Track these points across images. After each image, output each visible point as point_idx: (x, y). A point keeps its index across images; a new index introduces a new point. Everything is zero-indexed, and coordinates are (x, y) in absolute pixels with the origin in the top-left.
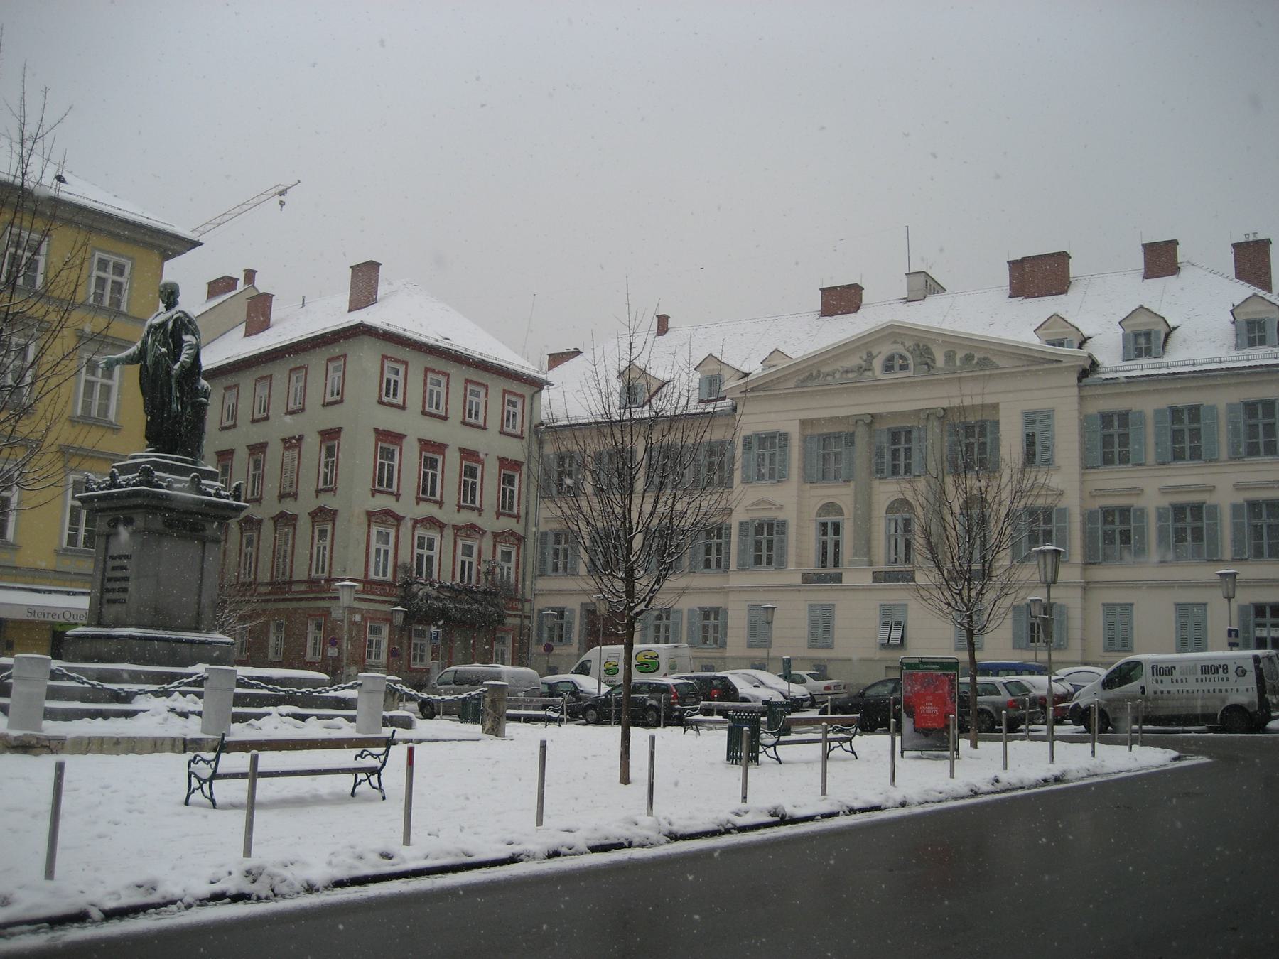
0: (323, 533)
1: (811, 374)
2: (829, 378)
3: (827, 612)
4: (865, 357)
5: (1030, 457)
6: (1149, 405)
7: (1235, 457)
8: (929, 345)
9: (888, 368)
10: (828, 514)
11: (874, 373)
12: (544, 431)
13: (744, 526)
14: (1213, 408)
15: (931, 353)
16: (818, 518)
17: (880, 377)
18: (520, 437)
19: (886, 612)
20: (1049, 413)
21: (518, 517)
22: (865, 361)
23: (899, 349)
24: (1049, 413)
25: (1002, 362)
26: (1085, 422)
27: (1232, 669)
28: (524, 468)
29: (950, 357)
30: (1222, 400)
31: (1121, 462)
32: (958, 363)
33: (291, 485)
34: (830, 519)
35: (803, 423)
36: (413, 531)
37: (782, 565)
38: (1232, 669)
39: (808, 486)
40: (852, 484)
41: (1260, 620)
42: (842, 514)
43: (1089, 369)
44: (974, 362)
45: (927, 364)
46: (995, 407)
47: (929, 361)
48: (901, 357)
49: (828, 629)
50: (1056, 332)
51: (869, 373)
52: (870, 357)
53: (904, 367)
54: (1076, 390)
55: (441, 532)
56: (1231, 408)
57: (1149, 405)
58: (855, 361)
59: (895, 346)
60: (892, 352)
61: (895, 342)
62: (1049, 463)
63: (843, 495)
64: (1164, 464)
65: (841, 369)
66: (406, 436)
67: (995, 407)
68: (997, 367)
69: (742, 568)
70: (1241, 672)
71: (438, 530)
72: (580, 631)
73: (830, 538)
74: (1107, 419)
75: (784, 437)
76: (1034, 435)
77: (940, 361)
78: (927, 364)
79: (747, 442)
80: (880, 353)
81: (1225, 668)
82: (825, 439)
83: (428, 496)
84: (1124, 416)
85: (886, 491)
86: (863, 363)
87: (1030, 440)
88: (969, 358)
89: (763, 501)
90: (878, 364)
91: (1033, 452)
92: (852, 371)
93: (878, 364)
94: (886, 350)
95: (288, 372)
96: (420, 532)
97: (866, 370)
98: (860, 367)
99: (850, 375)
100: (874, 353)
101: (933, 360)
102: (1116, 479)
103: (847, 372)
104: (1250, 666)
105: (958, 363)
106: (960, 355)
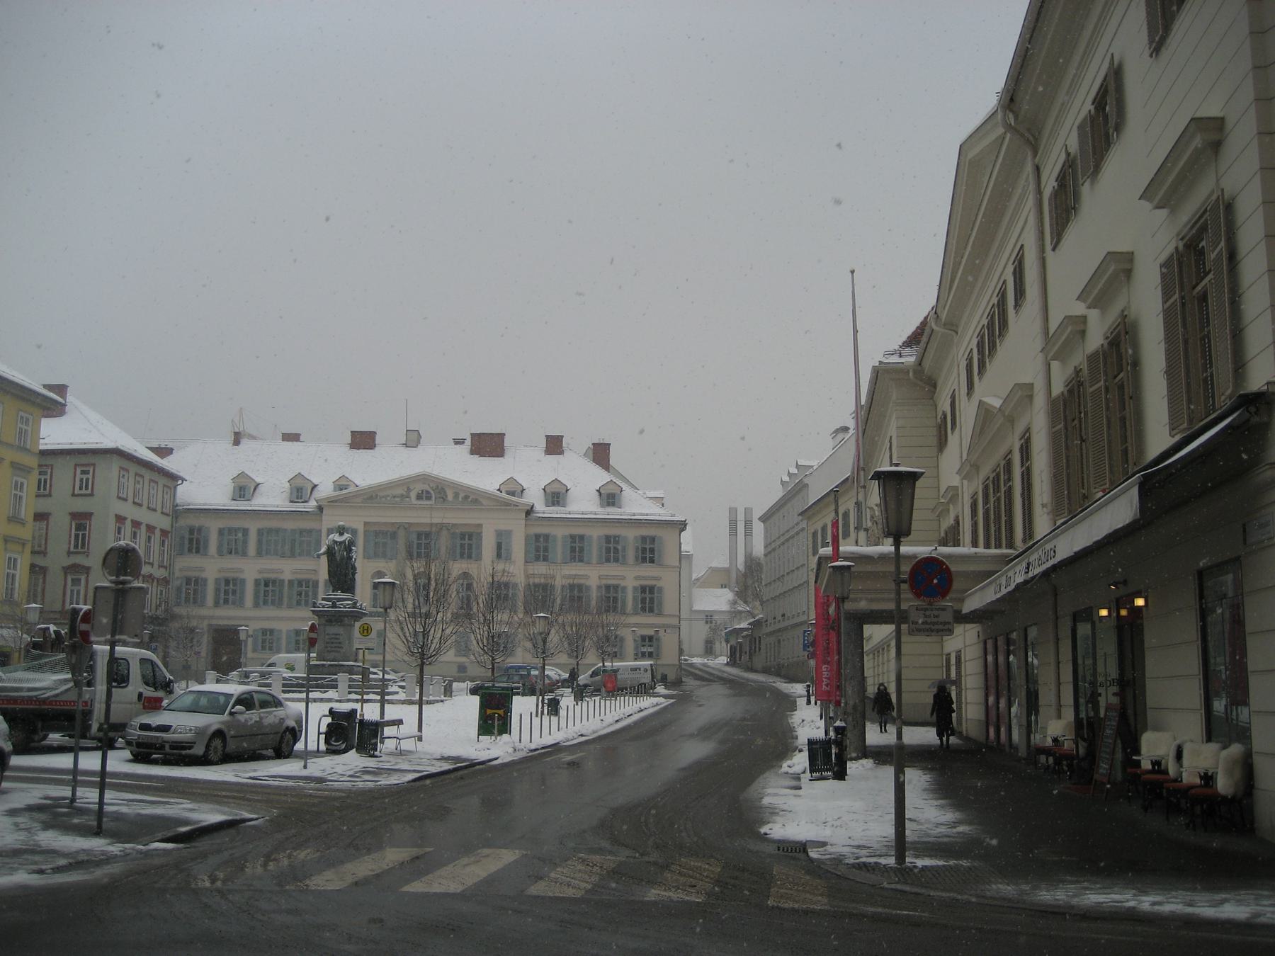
0: (76, 582)
2: (384, 499)
4: (406, 490)
5: (499, 556)
6: (560, 532)
7: (600, 563)
8: (446, 489)
9: (419, 497)
12: (177, 513)
14: (591, 537)
15: (445, 492)
17: (416, 502)
18: (168, 515)
20: (509, 533)
21: (166, 568)
23: (426, 487)
24: (509, 533)
25: (484, 502)
26: (527, 538)
27: (642, 669)
28: (170, 535)
29: (456, 495)
30: (595, 533)
32: (460, 499)
33: (40, 546)
35: (366, 524)
38: (642, 669)
39: (366, 560)
40: (394, 561)
43: (529, 512)
44: (470, 500)
46: (480, 526)
47: (444, 497)
50: (511, 487)
51: (408, 499)
52: (409, 490)
53: (429, 498)
56: (599, 537)
57: (560, 532)
58: (399, 491)
59: (425, 486)
61: (424, 483)
62: (508, 559)
64: (566, 563)
67: (480, 526)
68: (482, 505)
70: (646, 670)
74: (537, 537)
76: (501, 543)
77: (450, 497)
80: (414, 488)
81: (640, 669)
82: (377, 534)
83: (80, 549)
84: (547, 537)
86: (405, 493)
87: (499, 546)
88: (466, 497)
90: (413, 495)
91: (501, 551)
92: (398, 497)
93: (413, 495)
94: (419, 487)
98: (402, 495)
99: (397, 499)
100: (412, 488)
101: (446, 496)
102: (541, 568)
103: (394, 497)
104: (649, 668)
105: (460, 499)
106: (462, 495)
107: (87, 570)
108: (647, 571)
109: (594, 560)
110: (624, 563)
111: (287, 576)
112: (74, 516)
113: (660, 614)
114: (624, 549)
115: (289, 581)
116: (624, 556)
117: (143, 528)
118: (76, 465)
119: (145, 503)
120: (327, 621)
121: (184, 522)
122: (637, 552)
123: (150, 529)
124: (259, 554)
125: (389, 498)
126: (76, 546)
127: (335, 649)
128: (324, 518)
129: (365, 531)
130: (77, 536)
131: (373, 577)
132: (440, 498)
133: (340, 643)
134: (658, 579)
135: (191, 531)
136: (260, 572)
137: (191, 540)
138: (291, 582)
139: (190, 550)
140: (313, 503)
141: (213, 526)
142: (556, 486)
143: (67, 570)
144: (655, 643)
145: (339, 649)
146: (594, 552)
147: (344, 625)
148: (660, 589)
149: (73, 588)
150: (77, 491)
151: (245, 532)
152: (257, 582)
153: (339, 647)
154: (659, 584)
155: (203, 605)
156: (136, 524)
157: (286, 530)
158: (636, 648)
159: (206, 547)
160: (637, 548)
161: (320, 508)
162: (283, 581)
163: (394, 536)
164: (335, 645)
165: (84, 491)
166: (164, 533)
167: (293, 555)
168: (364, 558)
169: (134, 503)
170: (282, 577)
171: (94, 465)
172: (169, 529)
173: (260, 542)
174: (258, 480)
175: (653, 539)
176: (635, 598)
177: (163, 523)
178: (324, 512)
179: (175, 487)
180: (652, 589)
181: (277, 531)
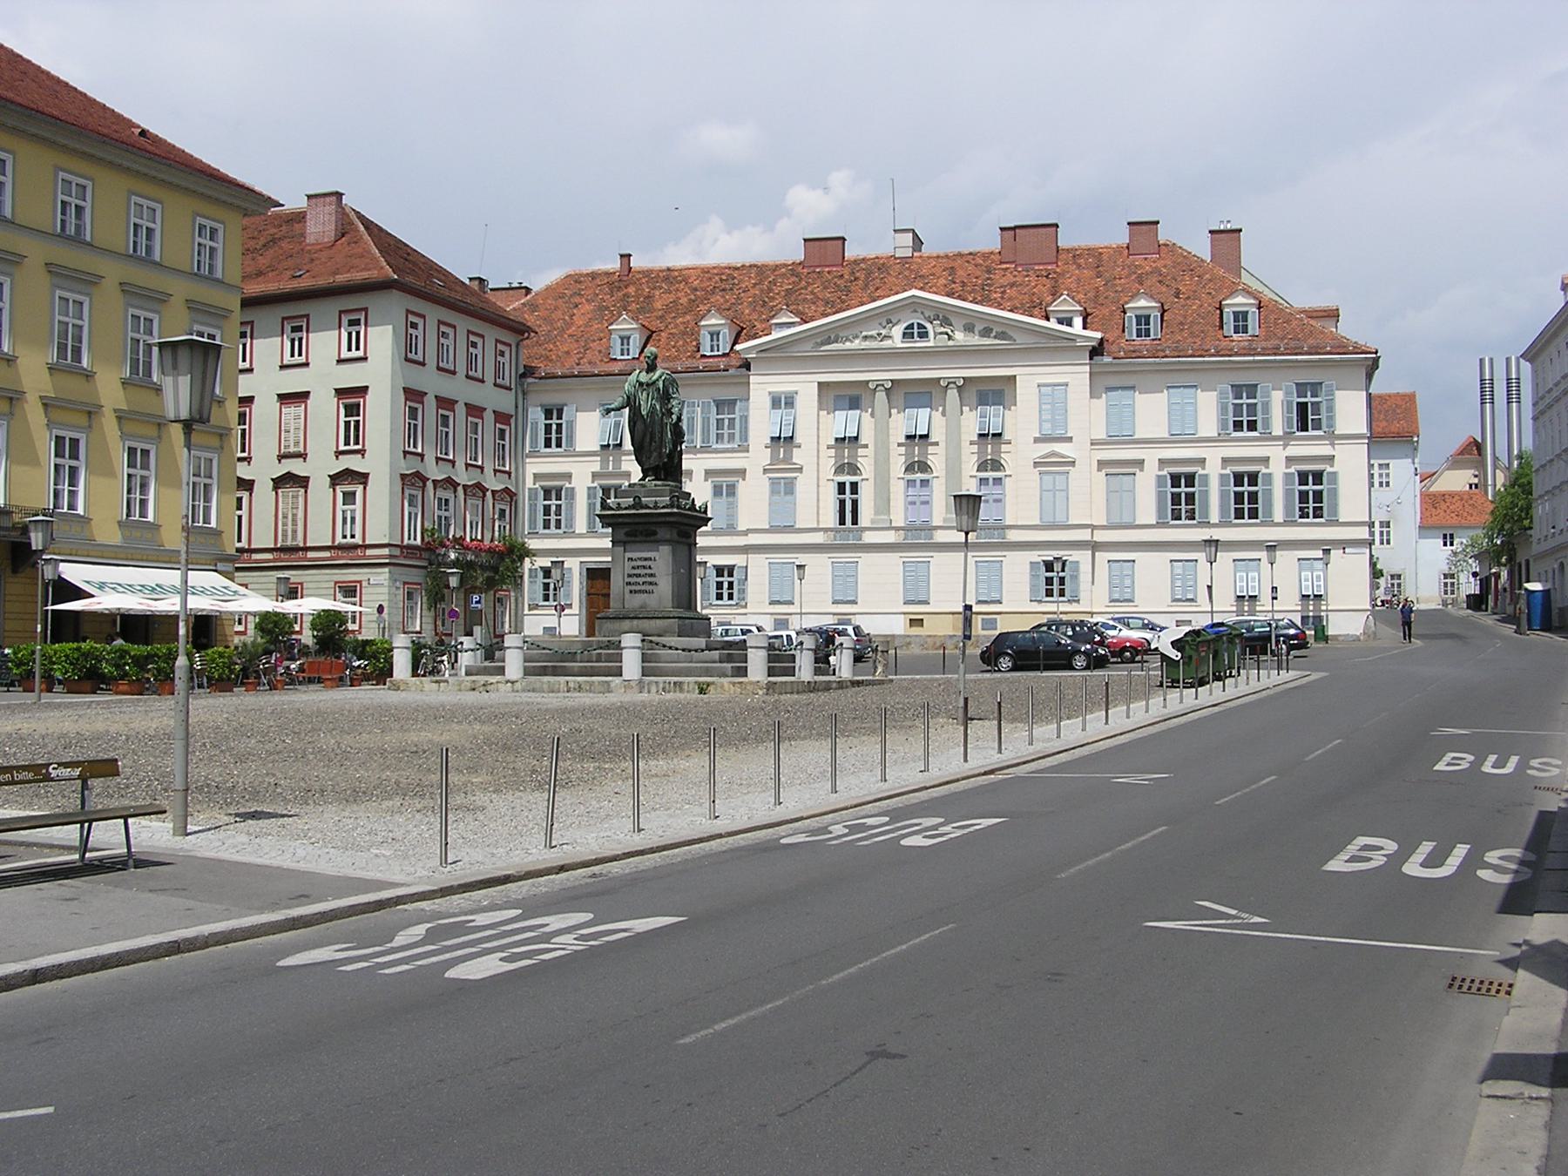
0: (349, 498)
9: (907, 334)
16: (835, 478)
28: (513, 421)
33: (297, 444)
34: (847, 479)
45: (947, 334)
47: (950, 333)
48: (920, 326)
51: (888, 343)
54: (1088, 368)
73: (848, 496)
95: (280, 320)
107: (363, 478)
112: (341, 393)
113: (1336, 523)
117: (460, 410)
118: (341, 312)
120: (627, 534)
123: (474, 411)
126: (347, 443)
127: (643, 588)
130: (347, 424)
132: (941, 333)
133: (652, 575)
143: (335, 479)
149: (346, 507)
150: (345, 354)
153: (651, 583)
156: (445, 403)
160: (1289, 403)
164: (644, 579)
165: (354, 354)
166: (501, 417)
169: (439, 369)
171: (366, 310)
176: (1288, 494)
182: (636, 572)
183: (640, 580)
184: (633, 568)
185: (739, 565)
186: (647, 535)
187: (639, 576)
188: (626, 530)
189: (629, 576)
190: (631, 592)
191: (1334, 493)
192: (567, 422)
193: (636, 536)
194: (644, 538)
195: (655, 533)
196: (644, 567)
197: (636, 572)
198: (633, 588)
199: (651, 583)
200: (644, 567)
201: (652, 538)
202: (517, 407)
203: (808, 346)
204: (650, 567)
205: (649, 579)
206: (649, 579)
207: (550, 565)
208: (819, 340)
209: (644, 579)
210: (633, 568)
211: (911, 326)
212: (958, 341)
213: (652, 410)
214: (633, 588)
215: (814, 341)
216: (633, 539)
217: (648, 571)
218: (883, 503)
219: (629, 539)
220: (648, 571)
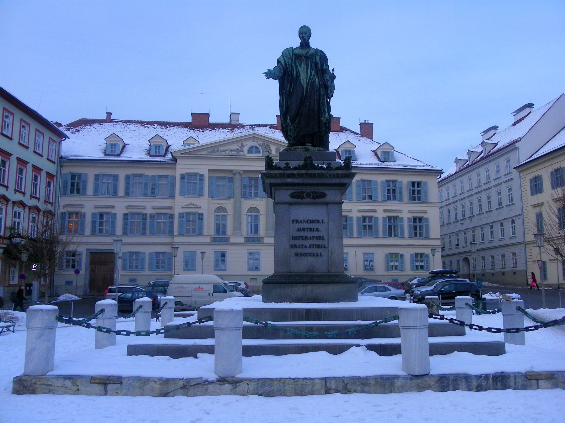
1: (215, 150)
2: (223, 153)
3: (223, 255)
4: (240, 145)
9: (250, 151)
10: (219, 212)
11: (244, 153)
12: (63, 161)
13: (181, 215)
14: (377, 181)
18: (54, 163)
19: (251, 254)
21: (51, 204)
22: (240, 147)
23: (255, 144)
28: (55, 179)
31: (255, 196)
35: (210, 171)
36: (13, 208)
37: (201, 234)
40: (232, 199)
41: (417, 259)
42: (226, 212)
45: (268, 152)
47: (270, 152)
48: (256, 147)
49: (224, 262)
51: (242, 153)
53: (259, 152)
55: (24, 209)
58: (235, 147)
59: (254, 143)
60: (253, 145)
61: (254, 141)
63: (229, 205)
65: (229, 149)
66: (12, 155)
69: (181, 234)
71: (23, 208)
72: (86, 263)
75: (201, 177)
78: (268, 152)
79: (183, 177)
80: (247, 145)
85: (247, 204)
86: (239, 148)
89: (191, 204)
90: (246, 149)
93: (246, 149)
94: (250, 144)
96: (16, 209)
97: (241, 151)
99: (233, 153)
100: (245, 144)
101: (271, 150)
108: (417, 206)
109: (380, 199)
110: (401, 201)
111: (149, 211)
113: (427, 238)
114: (400, 192)
115: (151, 214)
116: (401, 197)
119: (31, 146)
120: (293, 196)
121: (68, 170)
122: (410, 193)
124: (127, 193)
125: (227, 152)
127: (310, 250)
128: (178, 166)
129: (209, 177)
131: (215, 212)
133: (320, 238)
134: (425, 212)
135: (73, 176)
136: (128, 207)
137: (72, 185)
138: (152, 216)
139: (72, 192)
140: (169, 156)
141: (90, 173)
142: (348, 145)
144: (424, 258)
145: (318, 251)
146: (380, 193)
147: (327, 204)
148: (427, 220)
151: (116, 177)
152: (125, 216)
153: (319, 246)
154: (426, 216)
155: (82, 234)
157: (148, 176)
158: (412, 262)
159: (85, 187)
160: (410, 190)
161: (174, 159)
162: (145, 215)
163: (231, 180)
166: (50, 176)
167: (153, 194)
168: (209, 197)
170: (144, 211)
172: (55, 174)
173: (127, 185)
174: (126, 142)
175: (419, 184)
177: (52, 168)
178: (177, 163)
179: (60, 143)
180: (421, 219)
181: (141, 176)
182: (303, 234)
183: (307, 243)
184: (299, 230)
185: (168, 252)
186: (314, 198)
187: (306, 238)
188: (293, 191)
189: (294, 238)
190: (296, 255)
191: (427, 227)
192: (83, 182)
193: (302, 198)
194: (313, 201)
195: (323, 195)
196: (311, 230)
197: (303, 234)
198: (299, 251)
199: (319, 246)
200: (311, 230)
201: (322, 200)
202: (57, 172)
203: (204, 153)
204: (317, 230)
205: (316, 242)
206: (316, 242)
207: (112, 241)
208: (210, 151)
209: (310, 242)
210: (299, 230)
211: (252, 147)
212: (273, 154)
213: (311, 83)
214: (299, 251)
215: (207, 151)
216: (299, 200)
217: (316, 234)
218: (237, 227)
219: (295, 200)
220: (316, 234)
